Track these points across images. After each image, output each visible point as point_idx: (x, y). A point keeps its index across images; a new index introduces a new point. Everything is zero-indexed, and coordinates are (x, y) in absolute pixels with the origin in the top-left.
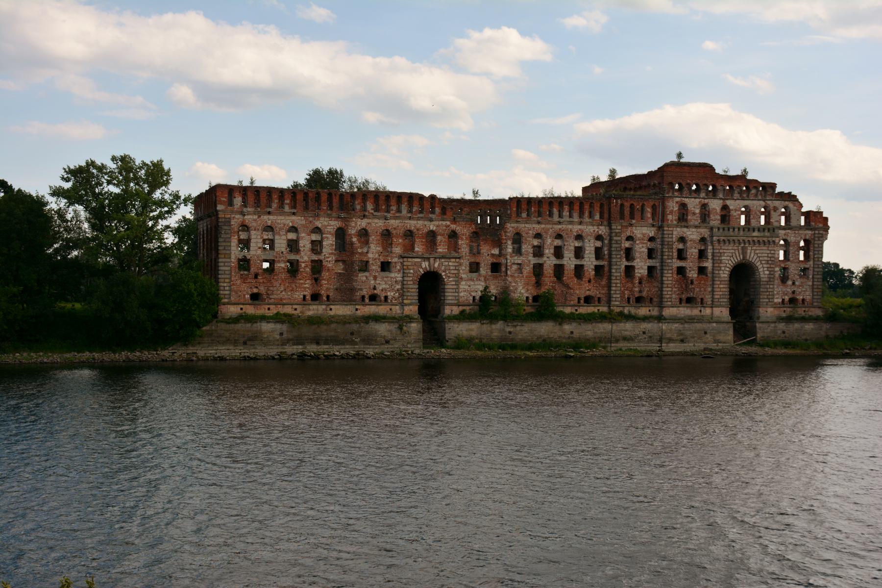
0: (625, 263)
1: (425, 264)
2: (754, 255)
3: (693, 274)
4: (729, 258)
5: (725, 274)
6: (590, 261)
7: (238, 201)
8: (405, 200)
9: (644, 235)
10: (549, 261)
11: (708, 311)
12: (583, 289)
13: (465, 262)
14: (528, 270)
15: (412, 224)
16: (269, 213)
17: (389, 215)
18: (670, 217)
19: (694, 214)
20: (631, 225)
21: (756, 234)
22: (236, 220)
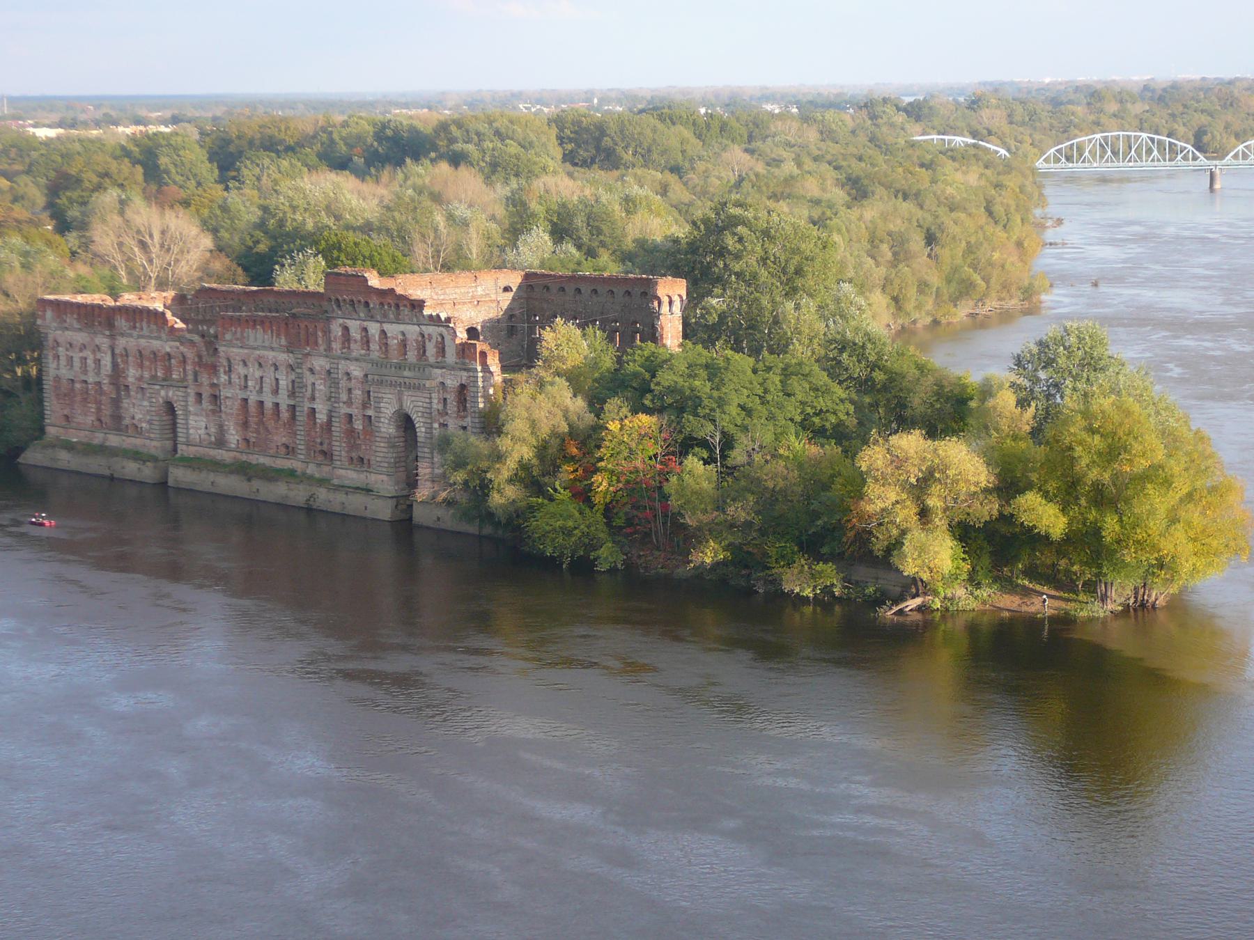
0: (307, 405)
1: (163, 393)
2: (414, 404)
3: (358, 425)
4: (389, 408)
5: (387, 428)
6: (284, 400)
7: (49, 314)
8: (145, 315)
9: (321, 367)
10: (253, 398)
11: (373, 478)
12: (280, 438)
13: (191, 391)
14: (237, 404)
15: (156, 344)
16: (67, 329)
17: (135, 333)
18: (334, 345)
19: (356, 341)
20: (308, 354)
21: (406, 373)
22: (51, 338)
